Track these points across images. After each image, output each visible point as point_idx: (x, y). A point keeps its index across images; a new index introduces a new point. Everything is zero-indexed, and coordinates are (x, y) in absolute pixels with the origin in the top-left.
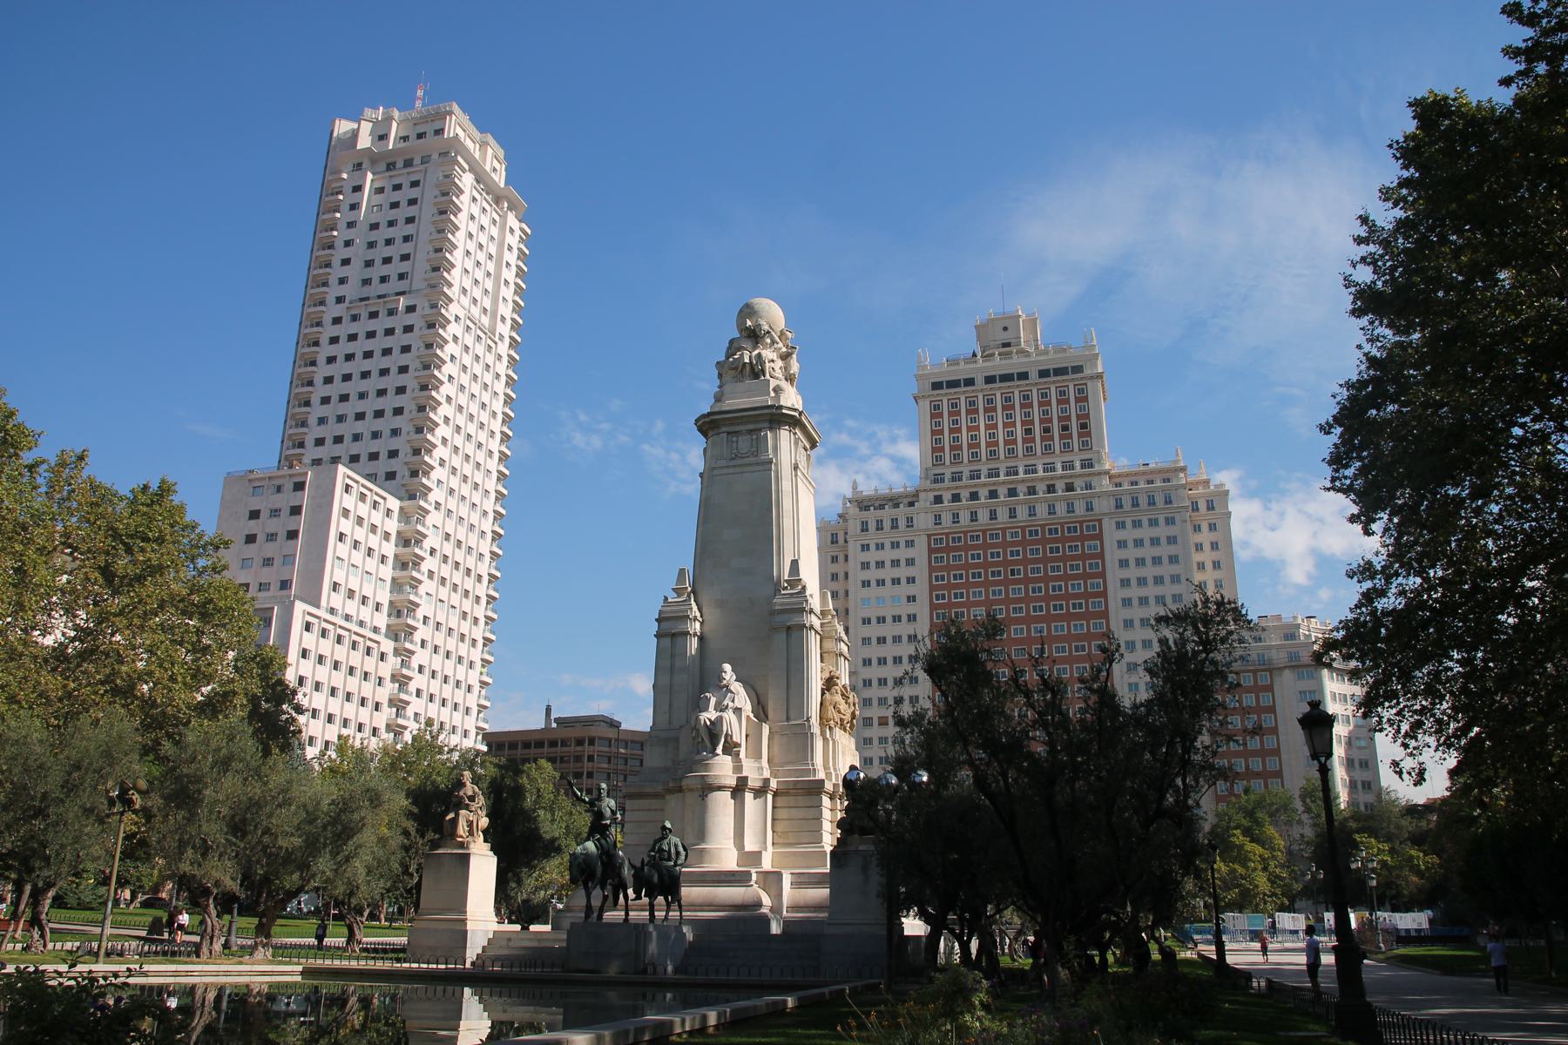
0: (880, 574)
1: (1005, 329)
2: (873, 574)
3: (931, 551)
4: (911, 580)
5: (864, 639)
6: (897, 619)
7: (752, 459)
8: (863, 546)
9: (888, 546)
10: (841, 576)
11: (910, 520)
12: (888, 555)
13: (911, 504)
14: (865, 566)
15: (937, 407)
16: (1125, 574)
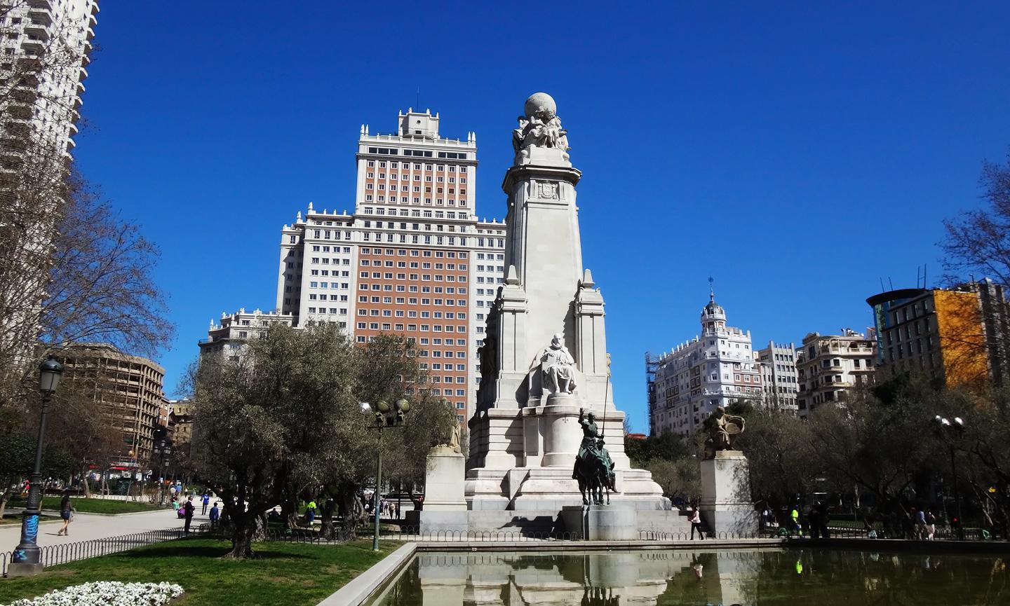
0: (325, 267)
1: (419, 122)
2: (320, 267)
3: (360, 256)
4: (346, 274)
5: (310, 309)
6: (334, 297)
7: (552, 201)
8: (314, 247)
9: (332, 248)
10: (295, 265)
11: (348, 234)
12: (331, 255)
13: (349, 224)
14: (316, 260)
15: (371, 164)
16: (481, 286)
